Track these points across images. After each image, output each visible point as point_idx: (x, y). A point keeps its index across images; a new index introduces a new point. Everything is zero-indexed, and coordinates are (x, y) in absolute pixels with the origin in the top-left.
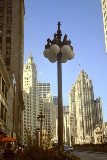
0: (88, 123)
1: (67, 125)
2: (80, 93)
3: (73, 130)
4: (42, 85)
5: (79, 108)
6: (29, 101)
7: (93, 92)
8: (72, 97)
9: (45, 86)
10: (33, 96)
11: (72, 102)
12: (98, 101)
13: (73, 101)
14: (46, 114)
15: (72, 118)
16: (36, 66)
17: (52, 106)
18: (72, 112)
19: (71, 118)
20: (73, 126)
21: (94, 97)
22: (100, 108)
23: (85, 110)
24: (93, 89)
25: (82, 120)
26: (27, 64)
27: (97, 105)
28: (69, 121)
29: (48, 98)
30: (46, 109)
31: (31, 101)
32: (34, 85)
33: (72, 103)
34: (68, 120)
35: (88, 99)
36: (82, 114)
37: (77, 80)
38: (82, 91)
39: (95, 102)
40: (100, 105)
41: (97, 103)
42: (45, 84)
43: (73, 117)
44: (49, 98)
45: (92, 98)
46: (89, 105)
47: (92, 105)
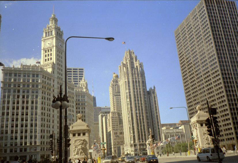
0: (141, 123)
1: (108, 129)
2: (127, 80)
3: (116, 135)
4: (72, 70)
5: (127, 102)
6: (50, 85)
7: (145, 80)
8: (114, 89)
9: (77, 72)
10: (57, 77)
11: (113, 96)
12: (152, 92)
13: (117, 94)
14: (79, 109)
15: (115, 118)
16: (62, 32)
17: (88, 97)
19: (113, 118)
20: (116, 129)
21: (146, 87)
23: (136, 104)
24: (144, 75)
25: (132, 119)
26: (47, 28)
27: (150, 97)
28: (111, 123)
29: (82, 85)
30: (79, 100)
31: (53, 85)
32: (59, 56)
33: (114, 98)
34: (109, 122)
35: (139, 89)
36: (131, 110)
37: (123, 63)
38: (130, 78)
39: (149, 93)
40: (155, 98)
41: (151, 94)
42: (77, 69)
43: (116, 117)
44: (84, 85)
45: (144, 88)
46: (141, 98)
47: (144, 98)
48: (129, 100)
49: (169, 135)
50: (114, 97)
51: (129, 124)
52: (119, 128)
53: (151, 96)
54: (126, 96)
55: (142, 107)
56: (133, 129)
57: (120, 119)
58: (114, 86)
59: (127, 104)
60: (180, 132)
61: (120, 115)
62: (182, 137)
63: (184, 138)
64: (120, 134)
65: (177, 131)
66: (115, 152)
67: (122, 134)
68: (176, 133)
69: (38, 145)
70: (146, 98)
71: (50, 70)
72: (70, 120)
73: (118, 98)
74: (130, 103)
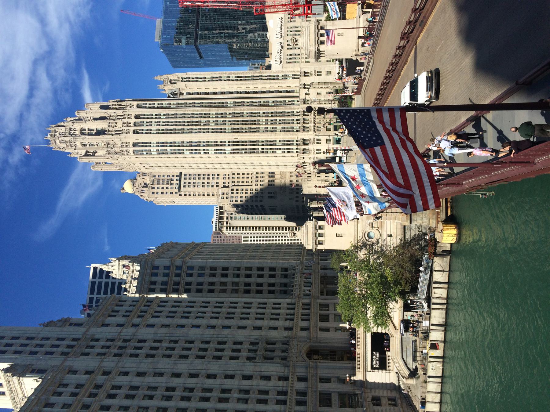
9: (100, 284)
11: (180, 195)
30: (164, 283)
31: (87, 373)
42: (93, 284)
58: (155, 191)
71: (30, 384)
72: (217, 315)
73: (184, 183)
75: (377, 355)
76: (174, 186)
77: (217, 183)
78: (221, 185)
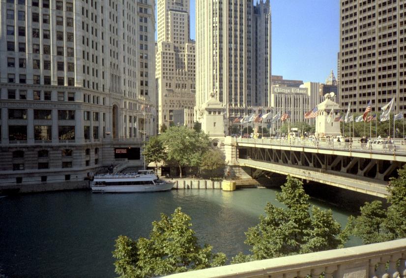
3: (168, 88)
5: (213, 23)
12: (262, 9)
15: (168, 56)
18: (168, 38)
19: (165, 56)
20: (170, 77)
22: (266, 29)
23: (230, 29)
27: (258, 19)
39: (256, 10)
40: (266, 23)
41: (260, 14)
43: (170, 54)
48: (217, 19)
49: (283, 97)
50: (169, 13)
51: (213, 69)
52: (174, 75)
53: (260, 16)
54: (213, 11)
55: (241, 37)
56: (221, 81)
57: (179, 59)
59: (214, 27)
60: (302, 94)
61: (178, 51)
62: (303, 103)
63: (307, 105)
64: (177, 86)
65: (298, 91)
66: (165, 118)
67: (179, 88)
68: (296, 96)
69: (79, 89)
70: (250, 20)
74: (219, 26)
75: (124, 151)
76: (174, 6)
77: (177, 42)
78: (176, 45)
